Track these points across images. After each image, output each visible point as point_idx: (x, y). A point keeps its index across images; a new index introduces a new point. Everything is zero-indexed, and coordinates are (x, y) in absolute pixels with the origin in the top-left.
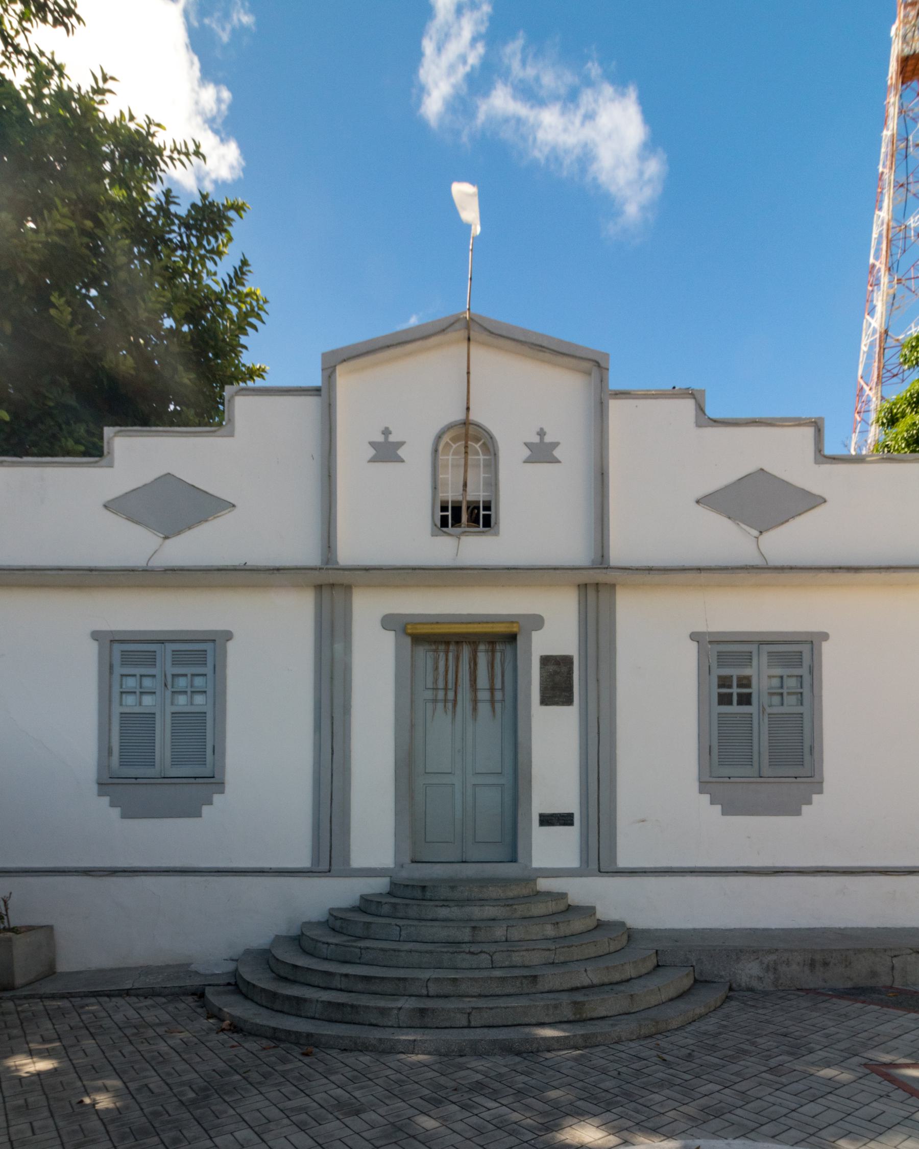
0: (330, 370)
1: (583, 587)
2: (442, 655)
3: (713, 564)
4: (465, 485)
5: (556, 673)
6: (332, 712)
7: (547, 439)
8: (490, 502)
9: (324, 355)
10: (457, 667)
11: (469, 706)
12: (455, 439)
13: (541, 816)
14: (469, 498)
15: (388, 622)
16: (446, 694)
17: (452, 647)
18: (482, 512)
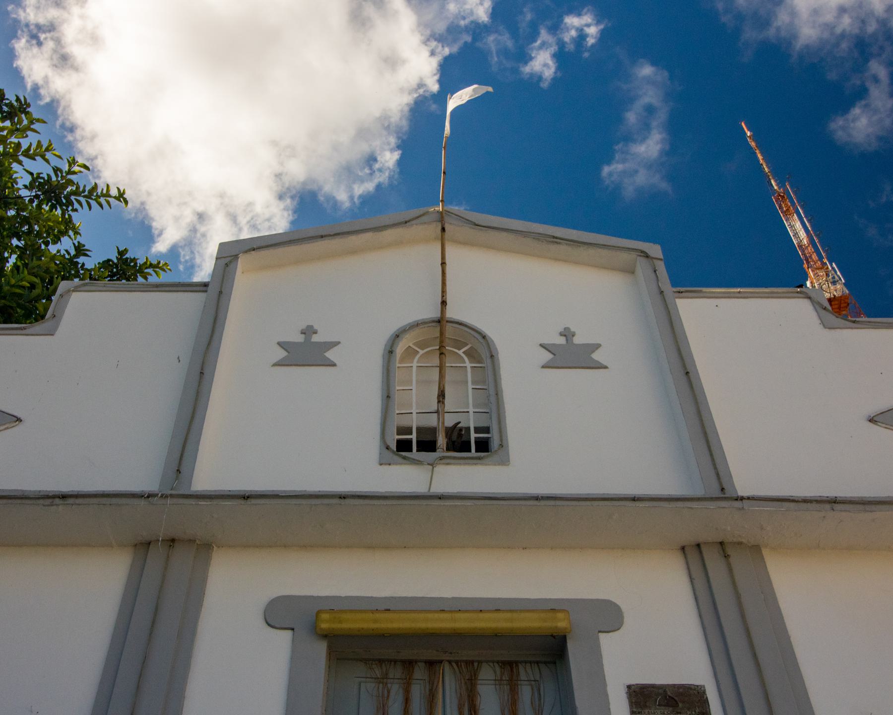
0: (228, 260)
15: (277, 614)
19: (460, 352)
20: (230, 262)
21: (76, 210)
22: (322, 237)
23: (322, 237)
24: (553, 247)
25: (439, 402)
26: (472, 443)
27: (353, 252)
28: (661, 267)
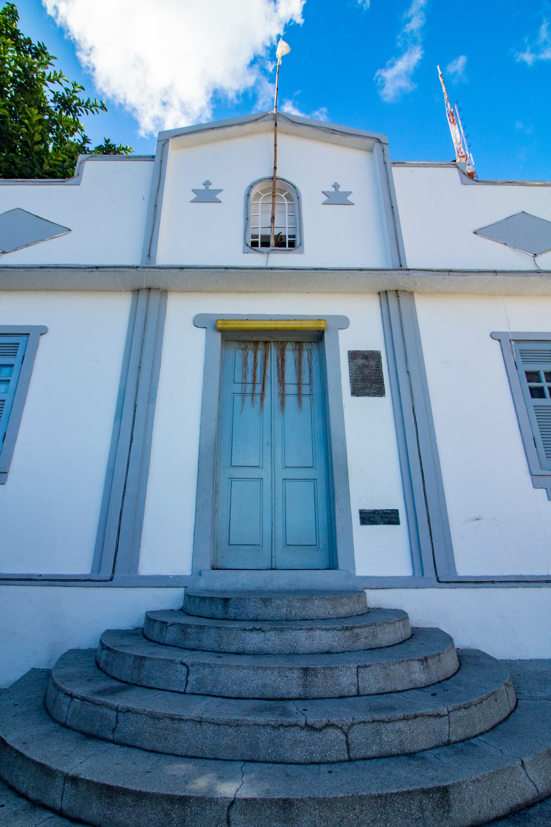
0: (164, 142)
1: (383, 294)
2: (251, 354)
5: (365, 366)
10: (265, 364)
13: (362, 512)
15: (199, 321)
19: (283, 196)
21: (80, 115)
22: (212, 128)
23: (212, 128)
24: (333, 136)
25: (272, 222)
27: (228, 138)
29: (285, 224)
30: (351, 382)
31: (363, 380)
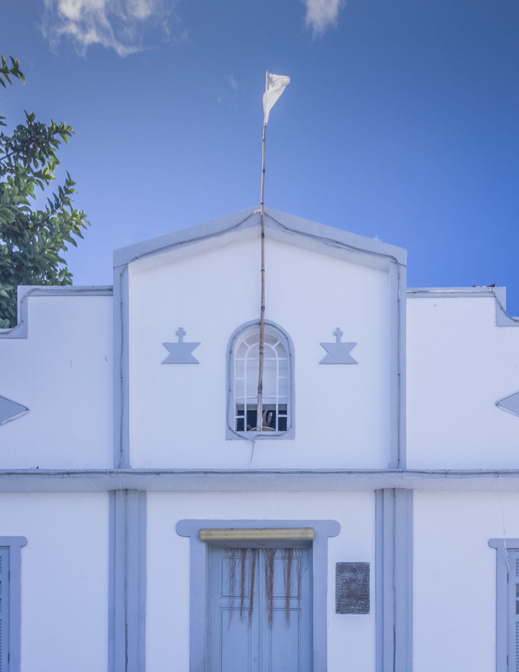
1: (380, 492)
3: (511, 467)
4: (260, 387)
5: (352, 580)
6: (126, 620)
7: (344, 339)
8: (286, 405)
9: (116, 252)
11: (265, 615)
12: (250, 341)
14: (265, 401)
15: (183, 528)
16: (242, 602)
17: (249, 554)
18: (278, 416)
20: (123, 271)
25: (259, 392)
26: (277, 420)
28: (404, 271)
29: (275, 395)
30: (336, 598)
31: (349, 596)
